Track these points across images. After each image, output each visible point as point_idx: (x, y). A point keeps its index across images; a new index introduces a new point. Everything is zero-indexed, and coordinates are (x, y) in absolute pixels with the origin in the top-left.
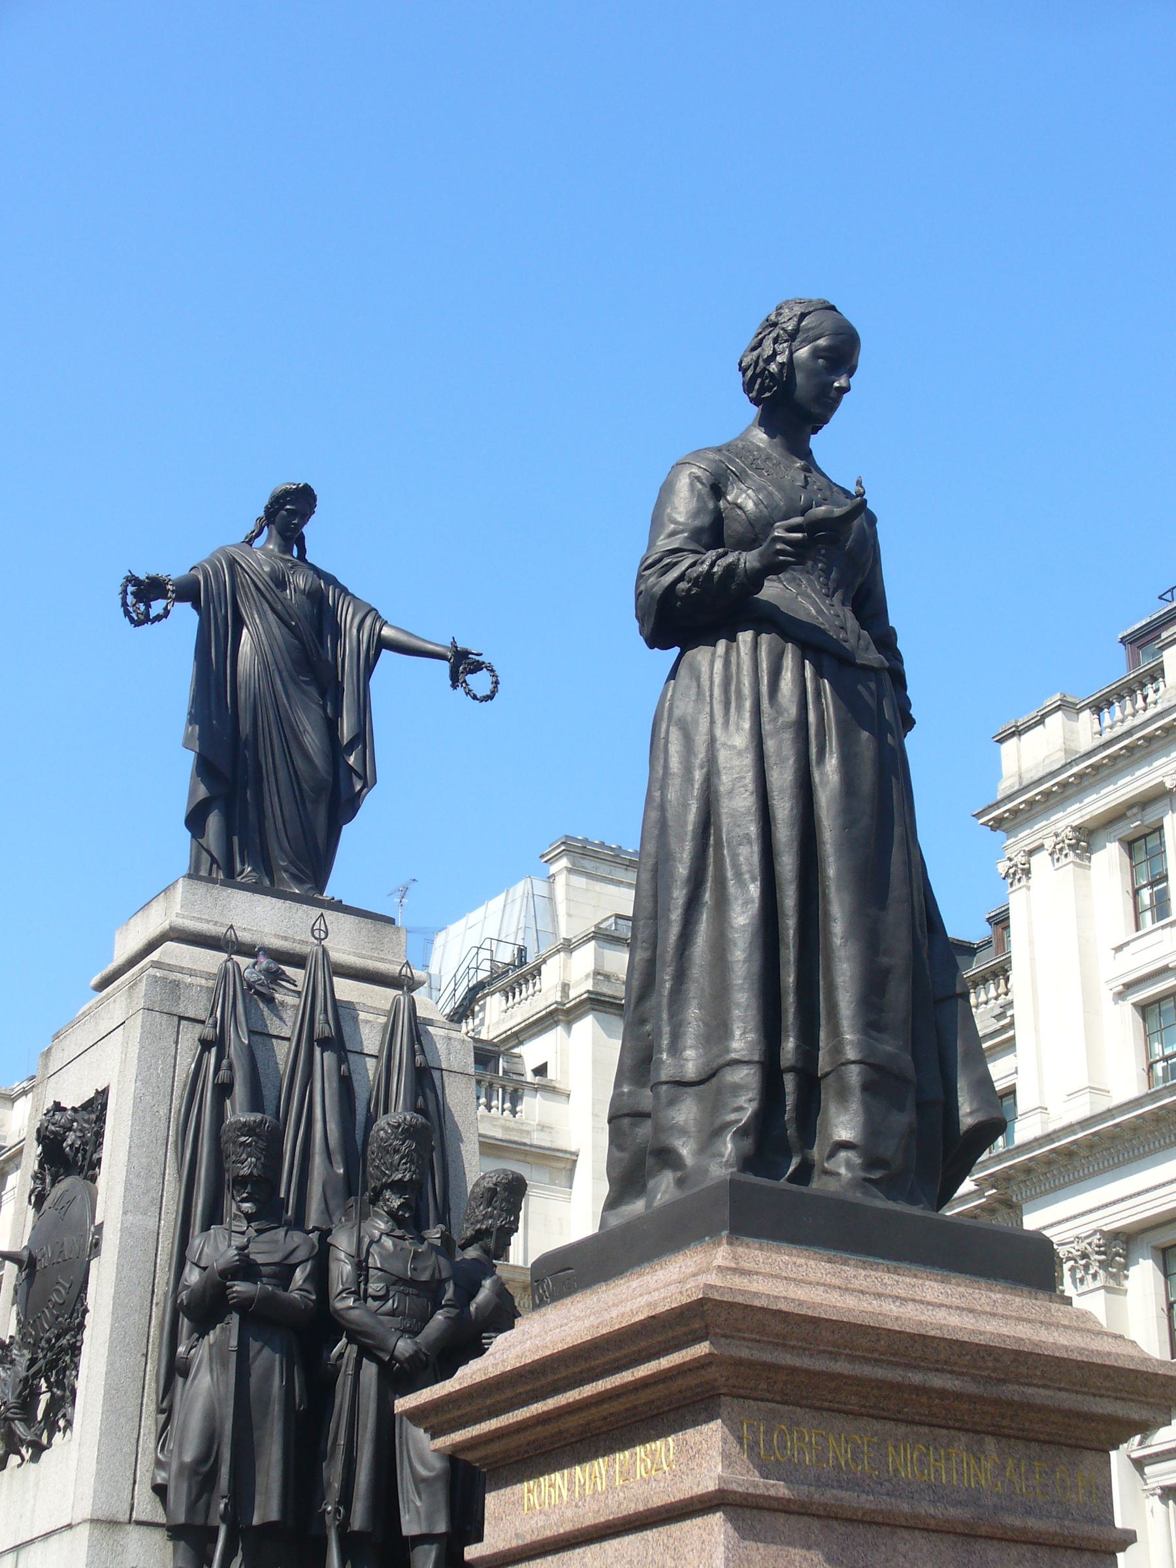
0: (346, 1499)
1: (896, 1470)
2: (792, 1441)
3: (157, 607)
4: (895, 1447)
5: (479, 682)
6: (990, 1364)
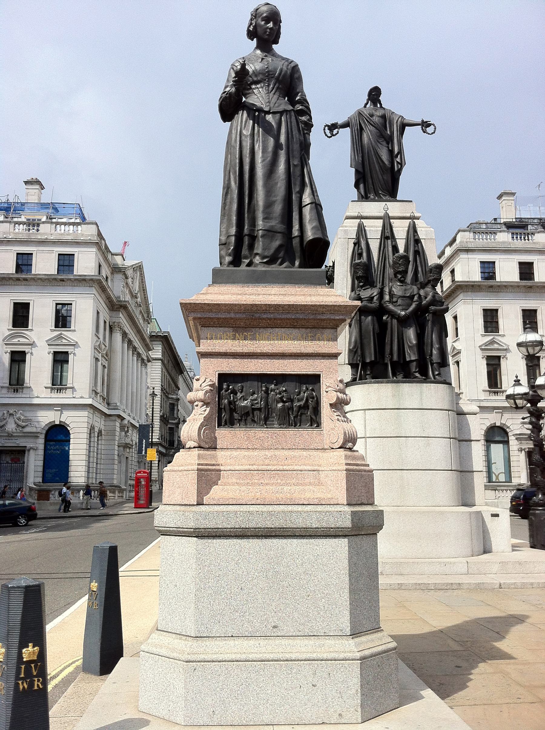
0: (391, 354)
3: (335, 132)
5: (430, 130)
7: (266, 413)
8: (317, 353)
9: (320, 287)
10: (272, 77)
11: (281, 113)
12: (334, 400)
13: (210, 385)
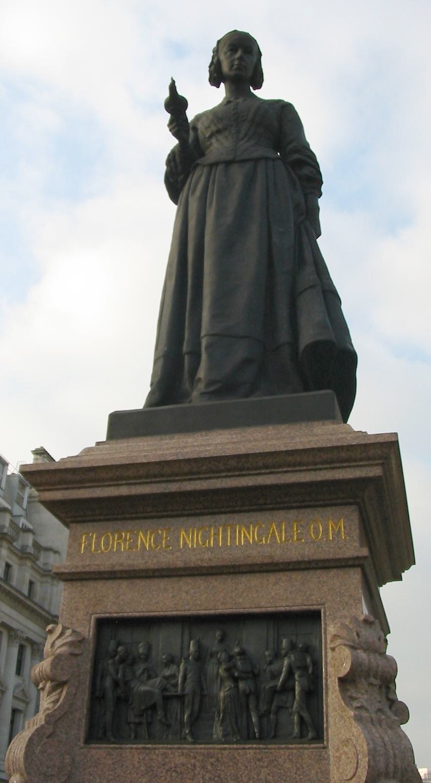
1: (185, 544)
2: (114, 539)
4: (186, 531)
6: (222, 468)
7: (196, 707)
8: (310, 562)
9: (321, 423)
10: (244, 121)
11: (256, 160)
12: (346, 668)
13: (71, 644)
